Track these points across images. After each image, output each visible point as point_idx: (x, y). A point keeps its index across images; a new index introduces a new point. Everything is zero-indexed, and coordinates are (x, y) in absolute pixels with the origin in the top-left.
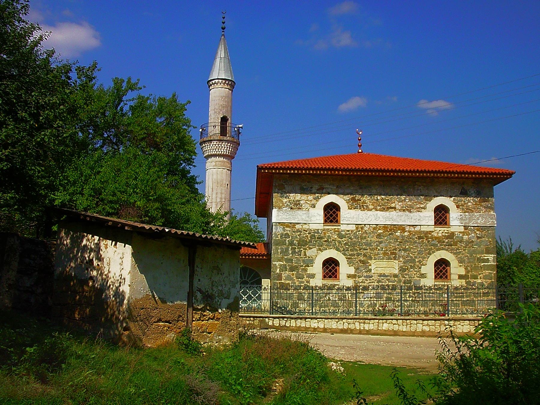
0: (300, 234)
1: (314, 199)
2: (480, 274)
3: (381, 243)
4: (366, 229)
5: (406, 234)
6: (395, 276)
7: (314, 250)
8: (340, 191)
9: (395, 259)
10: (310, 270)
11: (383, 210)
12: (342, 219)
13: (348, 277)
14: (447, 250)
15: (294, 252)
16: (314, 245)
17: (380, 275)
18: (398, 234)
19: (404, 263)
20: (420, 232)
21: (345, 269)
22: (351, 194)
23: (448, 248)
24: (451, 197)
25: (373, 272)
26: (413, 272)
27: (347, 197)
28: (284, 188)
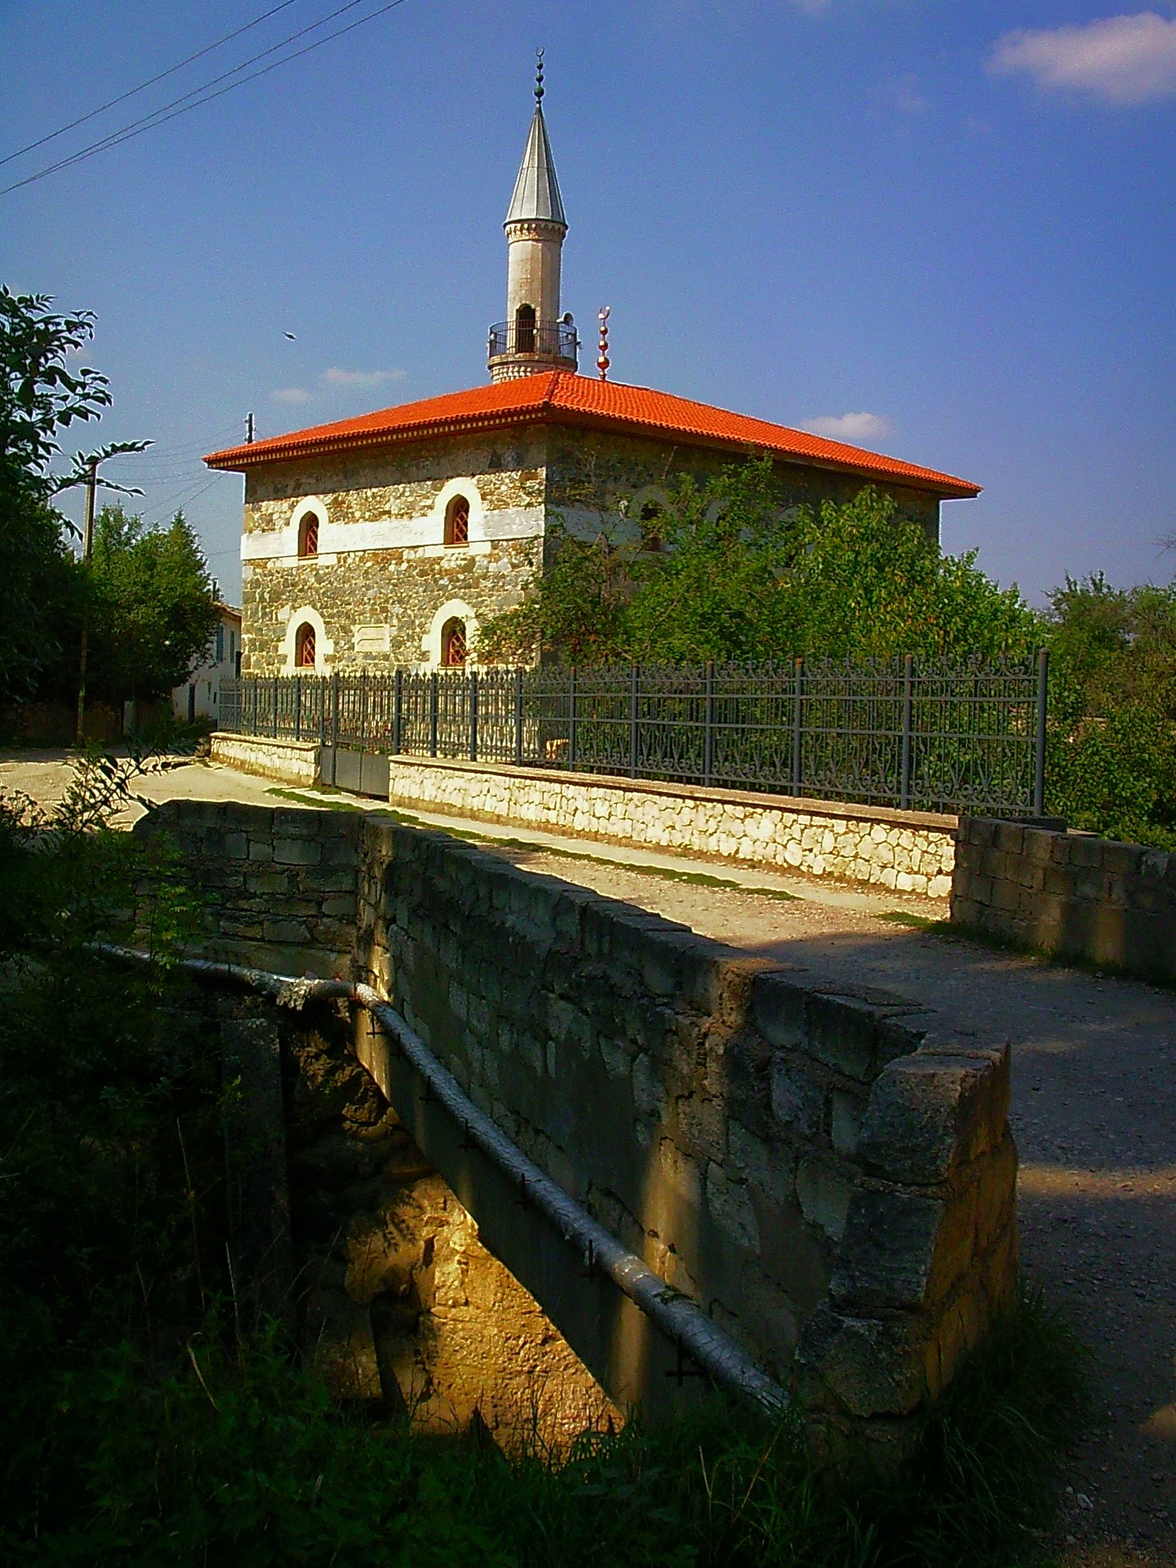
0: (271, 580)
3: (368, 587)
4: (350, 561)
5: (404, 566)
6: (386, 657)
8: (321, 486)
11: (375, 518)
15: (264, 615)
18: (392, 568)
19: (400, 629)
20: (423, 561)
21: (323, 646)
22: (334, 492)
23: (465, 594)
24: (473, 475)
27: (329, 498)
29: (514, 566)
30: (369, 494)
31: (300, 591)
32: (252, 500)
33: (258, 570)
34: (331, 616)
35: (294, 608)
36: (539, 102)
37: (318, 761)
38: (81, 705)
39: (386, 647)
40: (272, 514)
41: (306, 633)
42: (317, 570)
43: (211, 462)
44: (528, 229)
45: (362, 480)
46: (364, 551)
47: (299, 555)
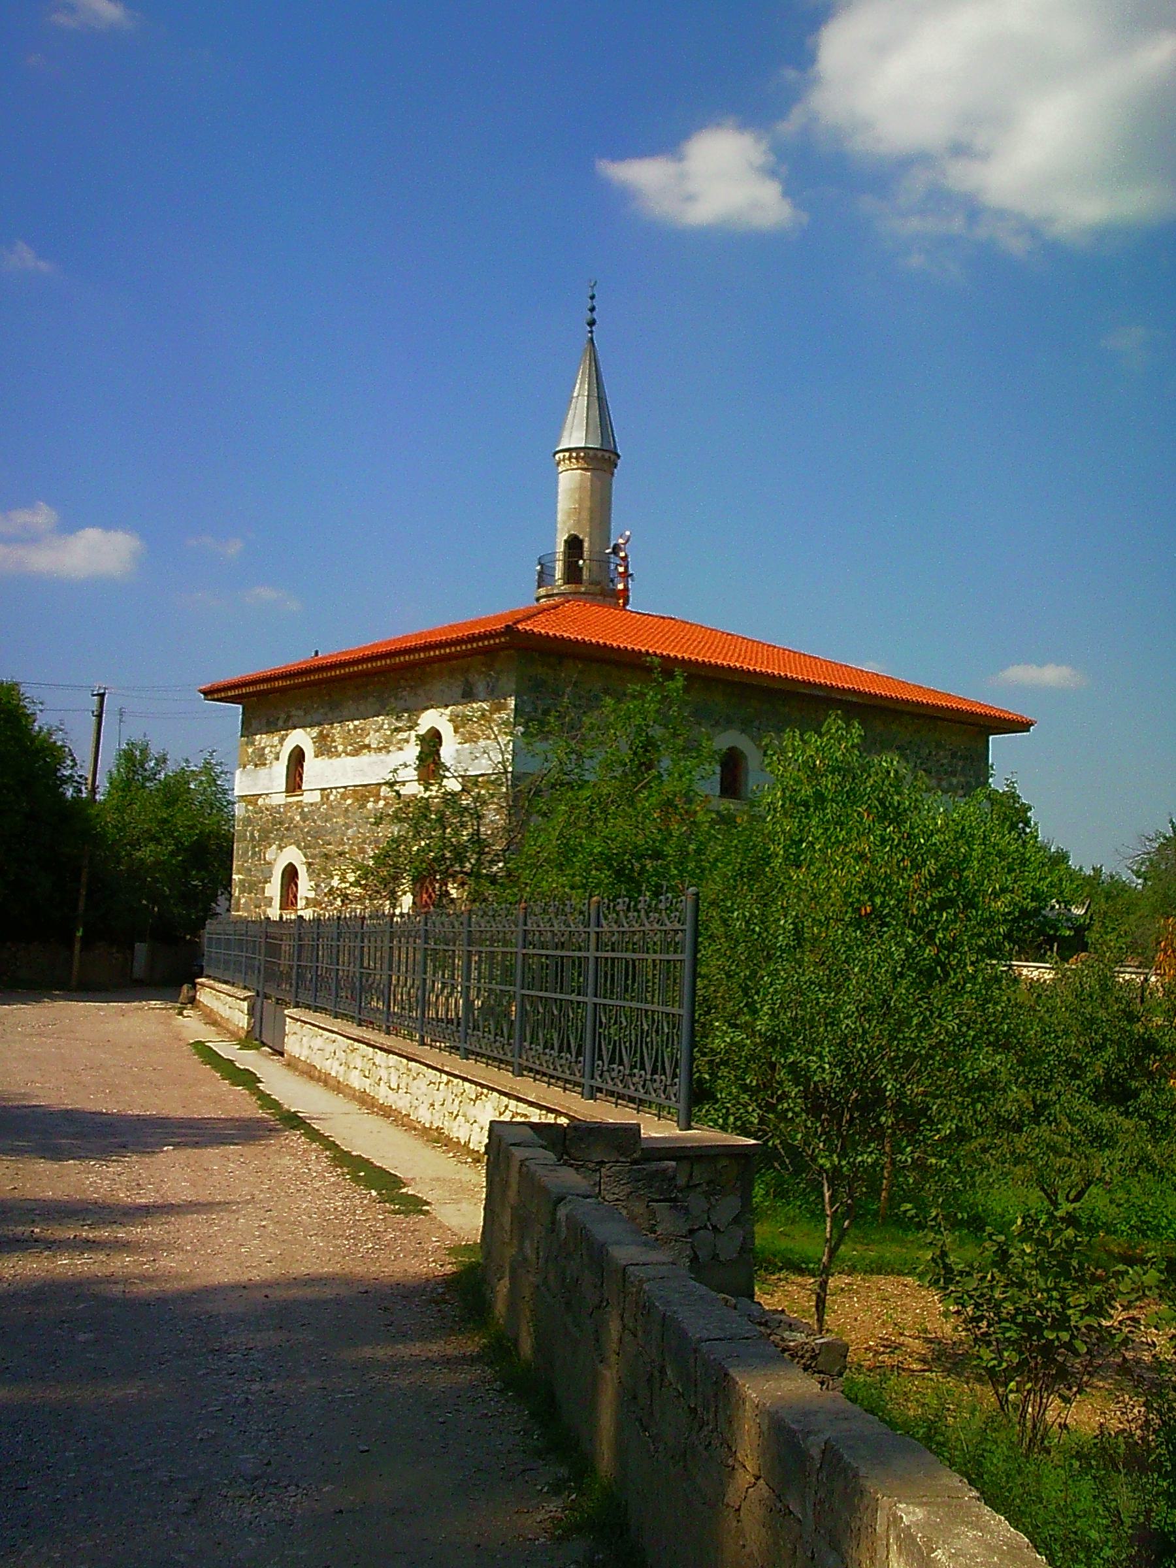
4: (332, 798)
5: (382, 803)
8: (309, 718)
11: (356, 753)
15: (254, 853)
18: (370, 805)
22: (320, 724)
24: (447, 706)
27: (315, 732)
30: (351, 727)
31: (287, 829)
32: (246, 733)
33: (250, 808)
34: (314, 857)
35: (281, 848)
36: (591, 332)
37: (251, 1012)
38: (77, 947)
40: (264, 748)
41: (290, 874)
42: (303, 808)
43: (208, 693)
44: (576, 458)
45: (346, 712)
46: (345, 787)
47: (287, 791)
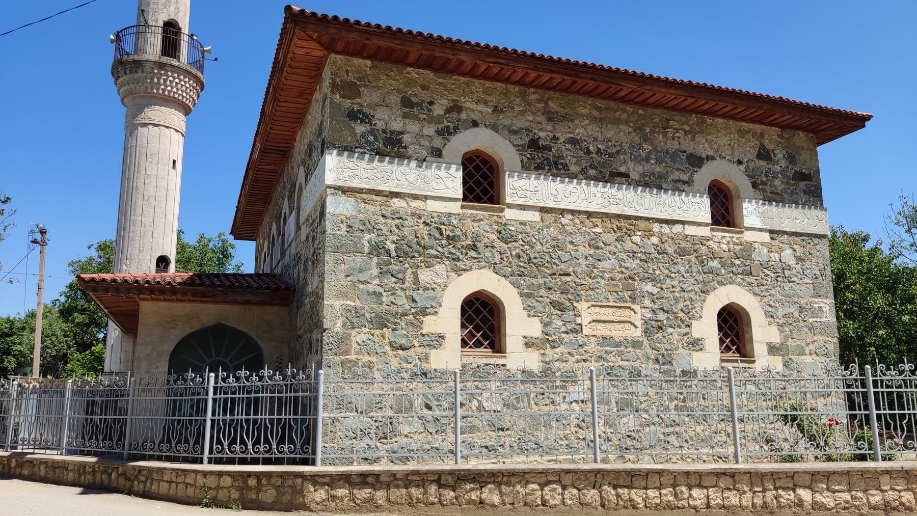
1: (439, 133)
2: (808, 345)
5: (655, 240)
6: (636, 344)
7: (440, 268)
9: (633, 299)
10: (430, 325)
12: (508, 191)
13: (527, 345)
14: (740, 285)
16: (440, 257)
17: (604, 340)
18: (637, 239)
21: (519, 324)
25: (586, 331)
26: (674, 334)
28: (359, 95)
29: (799, 259)
39: (638, 333)
